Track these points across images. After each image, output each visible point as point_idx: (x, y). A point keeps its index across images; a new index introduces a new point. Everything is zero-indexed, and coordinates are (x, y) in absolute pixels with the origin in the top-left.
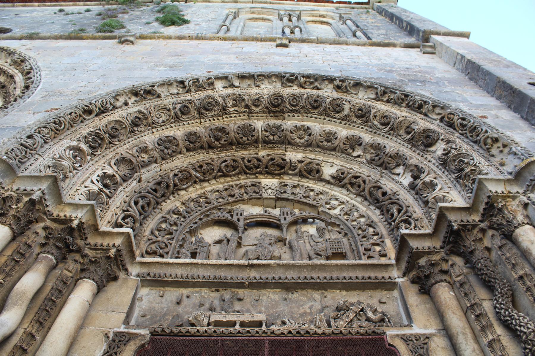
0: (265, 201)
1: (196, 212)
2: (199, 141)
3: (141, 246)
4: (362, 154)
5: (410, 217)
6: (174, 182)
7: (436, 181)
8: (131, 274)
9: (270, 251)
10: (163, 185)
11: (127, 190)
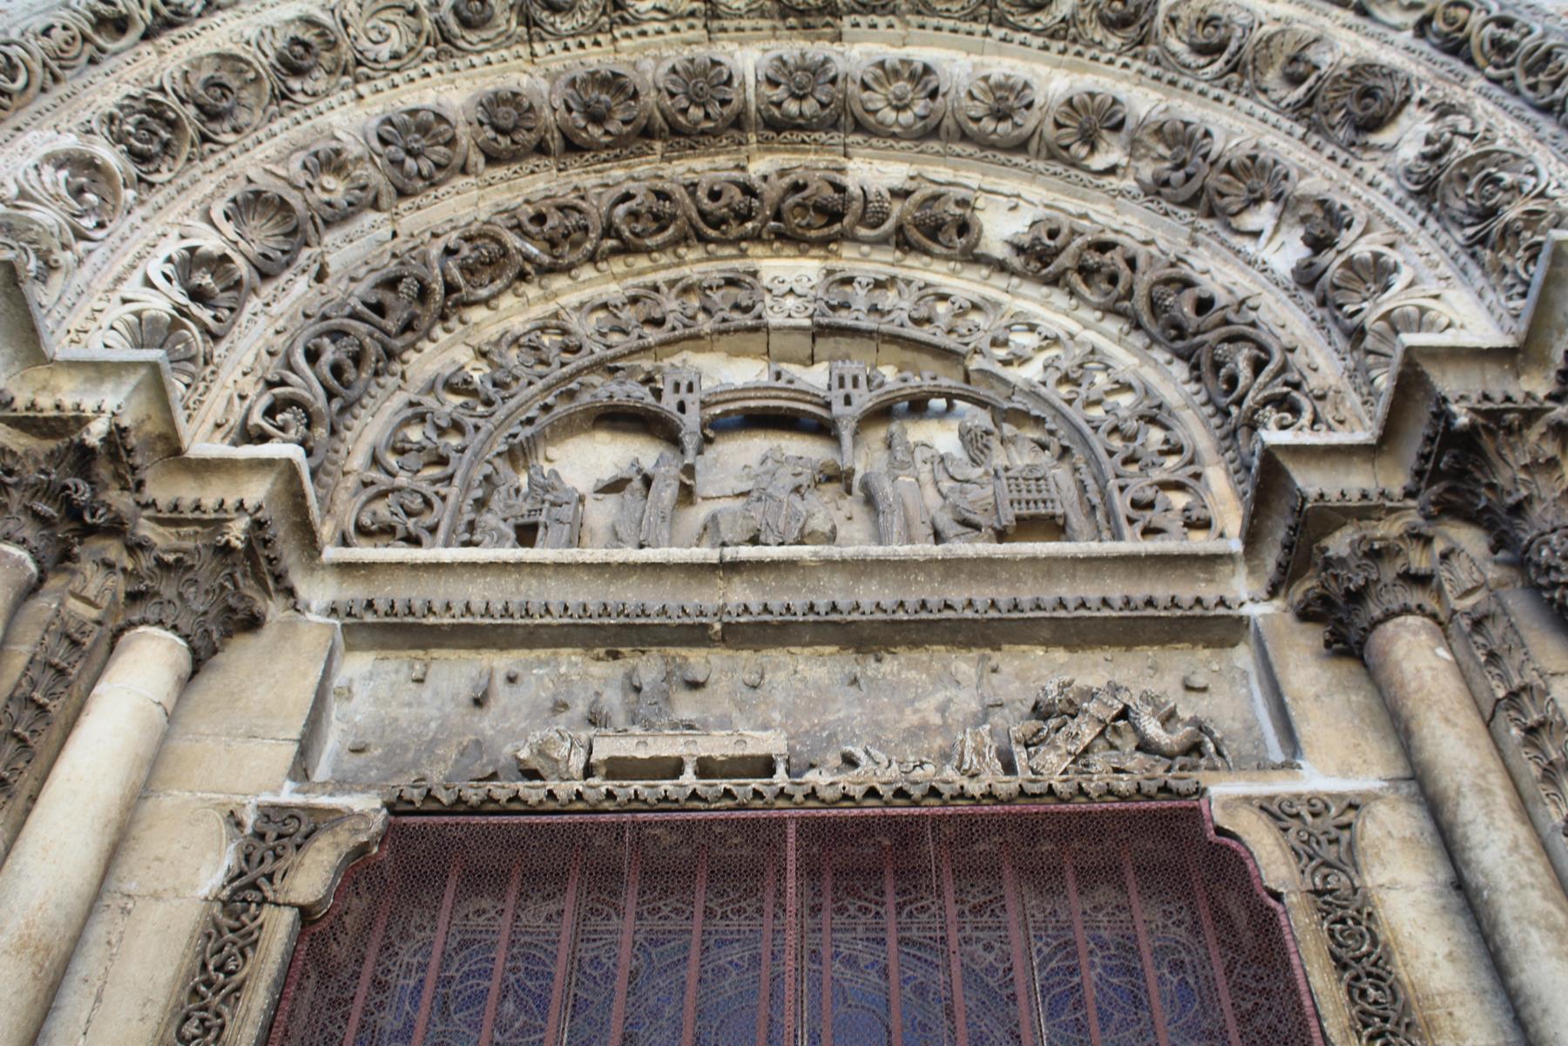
0: (774, 338)
1: (530, 383)
2: (530, 124)
3: (339, 507)
4: (1124, 161)
5: (1296, 386)
6: (444, 276)
7: (1392, 256)
8: (308, 607)
9: (796, 515)
11: (275, 309)
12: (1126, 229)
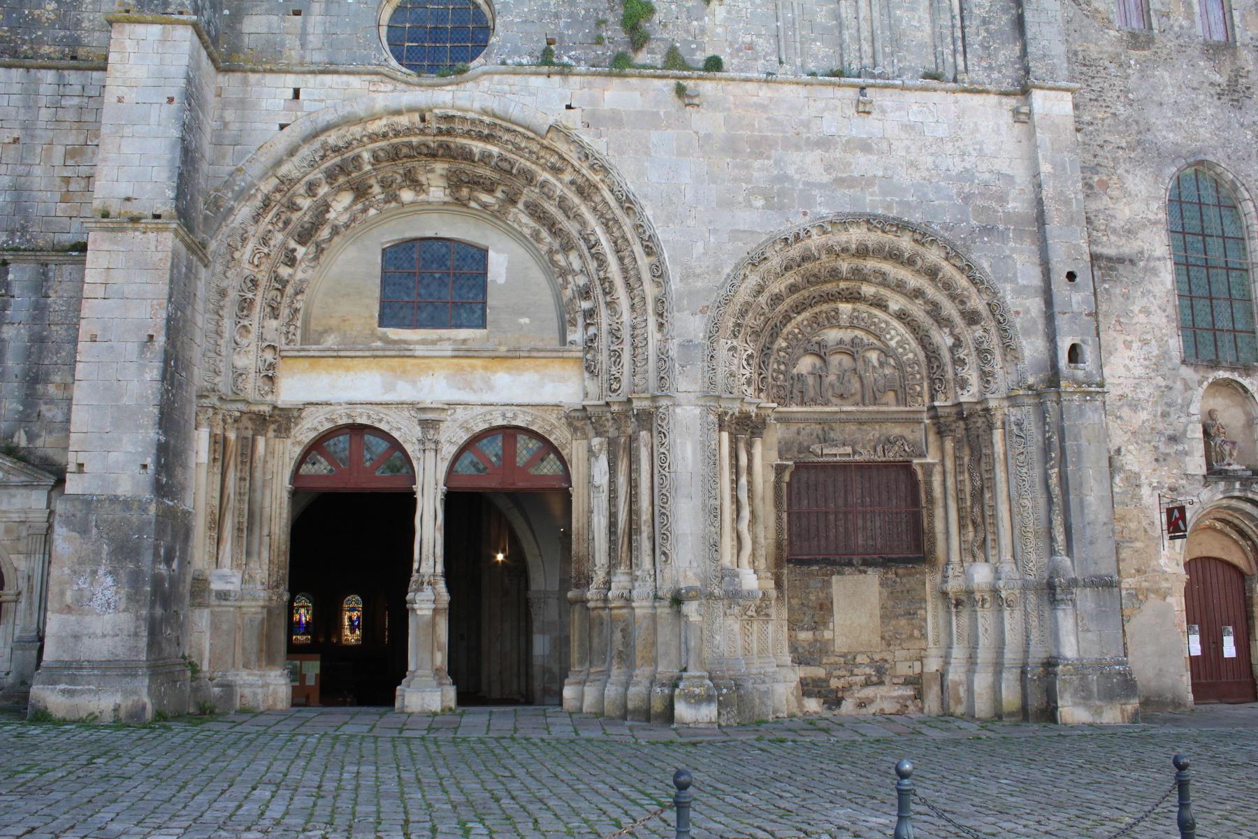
7: (967, 361)
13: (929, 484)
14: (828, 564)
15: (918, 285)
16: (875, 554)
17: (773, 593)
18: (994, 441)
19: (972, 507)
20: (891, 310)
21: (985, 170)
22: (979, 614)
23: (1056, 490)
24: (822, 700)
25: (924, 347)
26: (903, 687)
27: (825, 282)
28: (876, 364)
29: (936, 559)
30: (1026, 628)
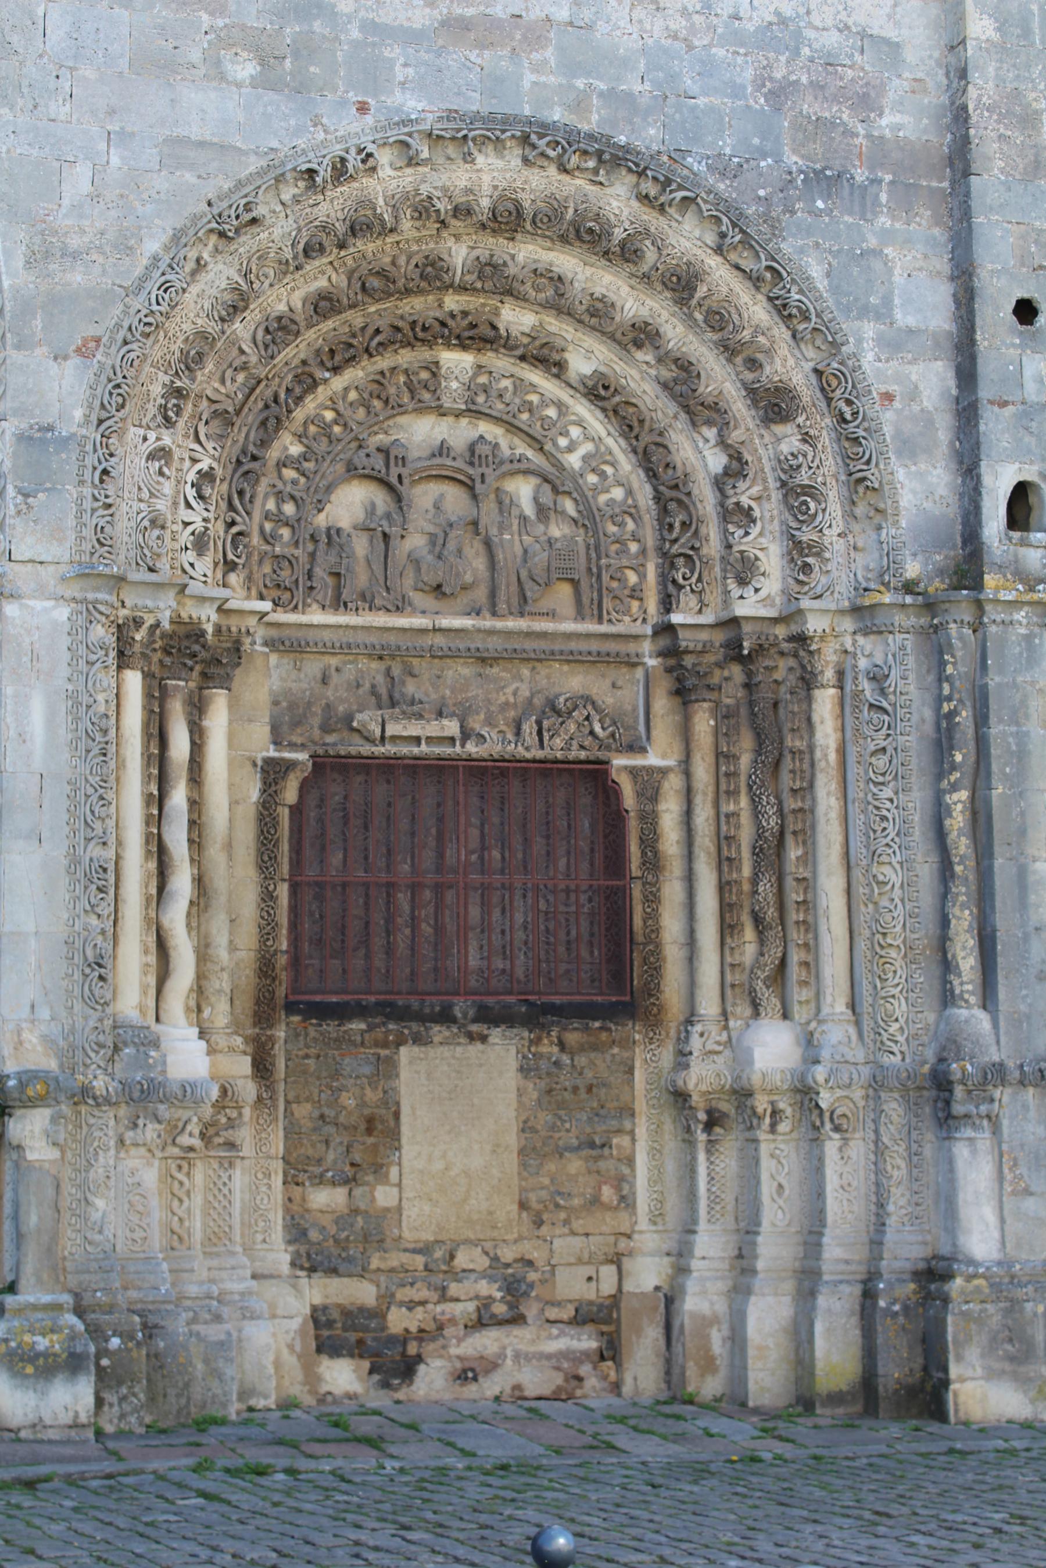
7: (757, 513)
10: (272, 421)
12: (645, 397)
13: (650, 820)
14: (389, 1017)
15: (644, 312)
16: (510, 993)
17: (248, 1090)
18: (816, 718)
19: (755, 881)
20: (572, 375)
21: (829, 23)
22: (764, 1149)
23: (962, 845)
24: (366, 1364)
25: (652, 474)
26: (572, 1331)
27: (408, 292)
28: (529, 510)
29: (661, 1008)
30: (877, 1184)
